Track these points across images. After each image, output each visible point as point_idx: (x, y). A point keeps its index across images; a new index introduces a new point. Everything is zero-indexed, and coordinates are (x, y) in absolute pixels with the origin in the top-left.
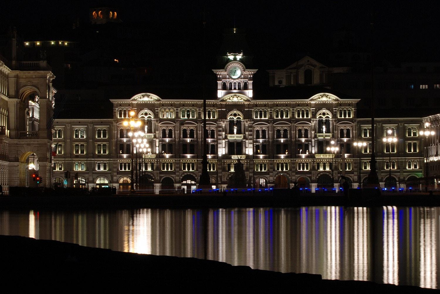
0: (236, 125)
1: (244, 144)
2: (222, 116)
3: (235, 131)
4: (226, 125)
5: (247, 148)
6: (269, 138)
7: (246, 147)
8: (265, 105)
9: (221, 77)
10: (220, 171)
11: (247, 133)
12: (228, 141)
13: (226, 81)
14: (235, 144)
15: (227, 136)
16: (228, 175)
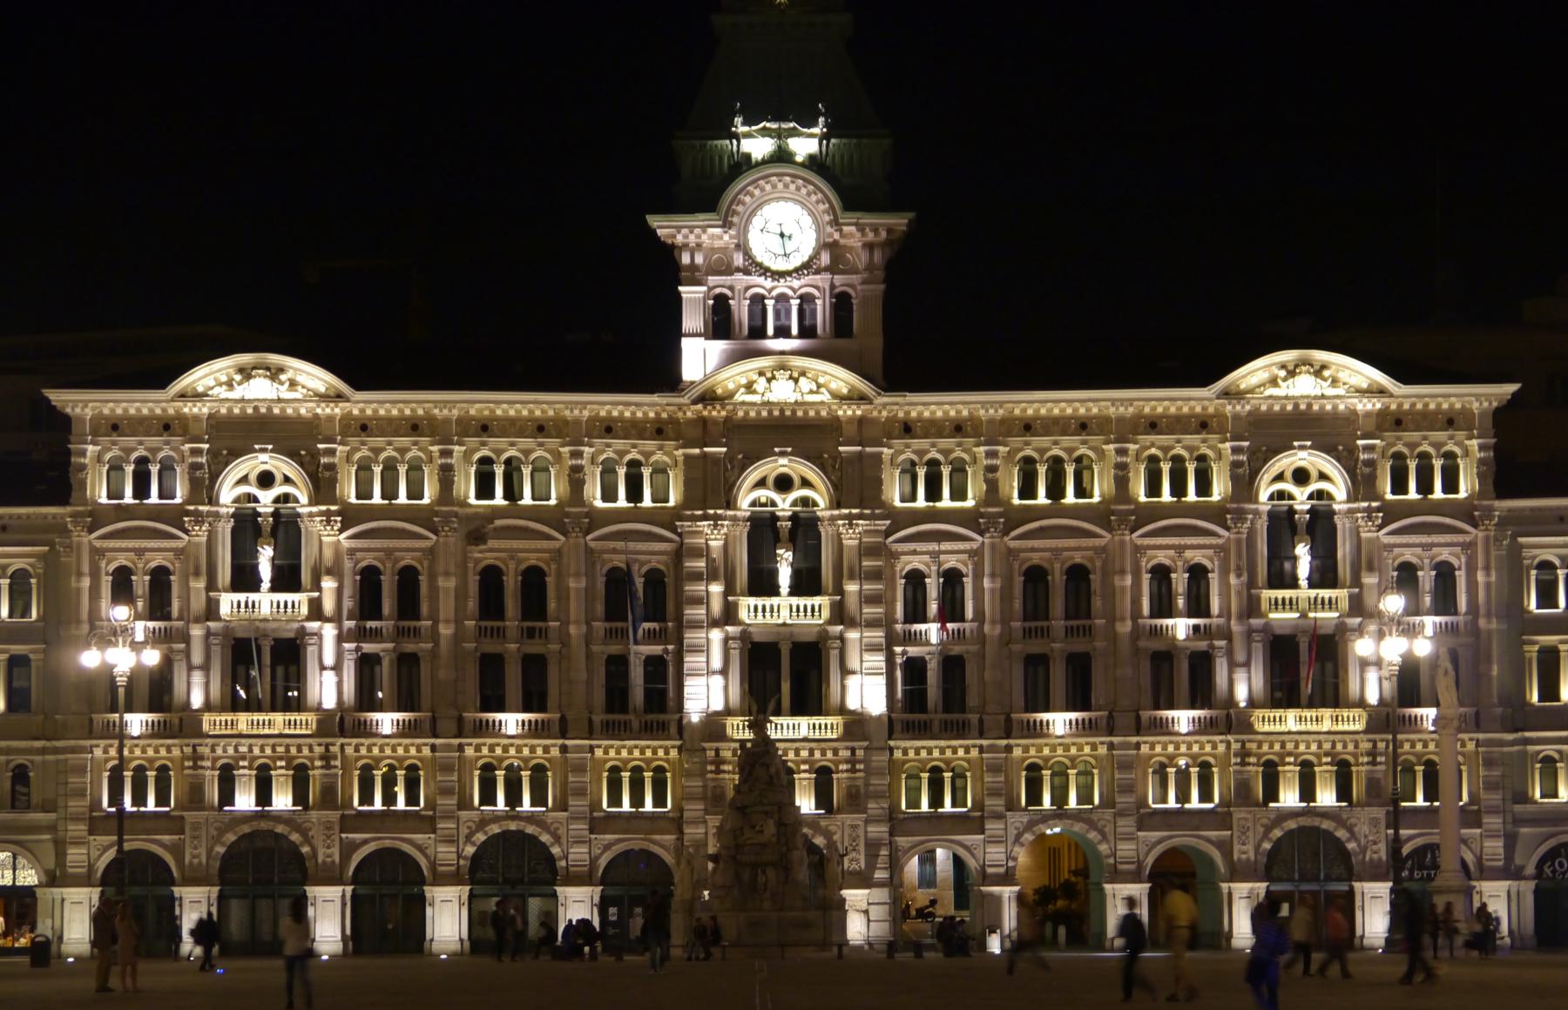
0: (793, 540)
1: (834, 654)
2: (711, 489)
4: (730, 540)
5: (854, 673)
6: (979, 616)
7: (846, 672)
9: (699, 259)
11: (851, 588)
13: (731, 288)
15: (736, 605)
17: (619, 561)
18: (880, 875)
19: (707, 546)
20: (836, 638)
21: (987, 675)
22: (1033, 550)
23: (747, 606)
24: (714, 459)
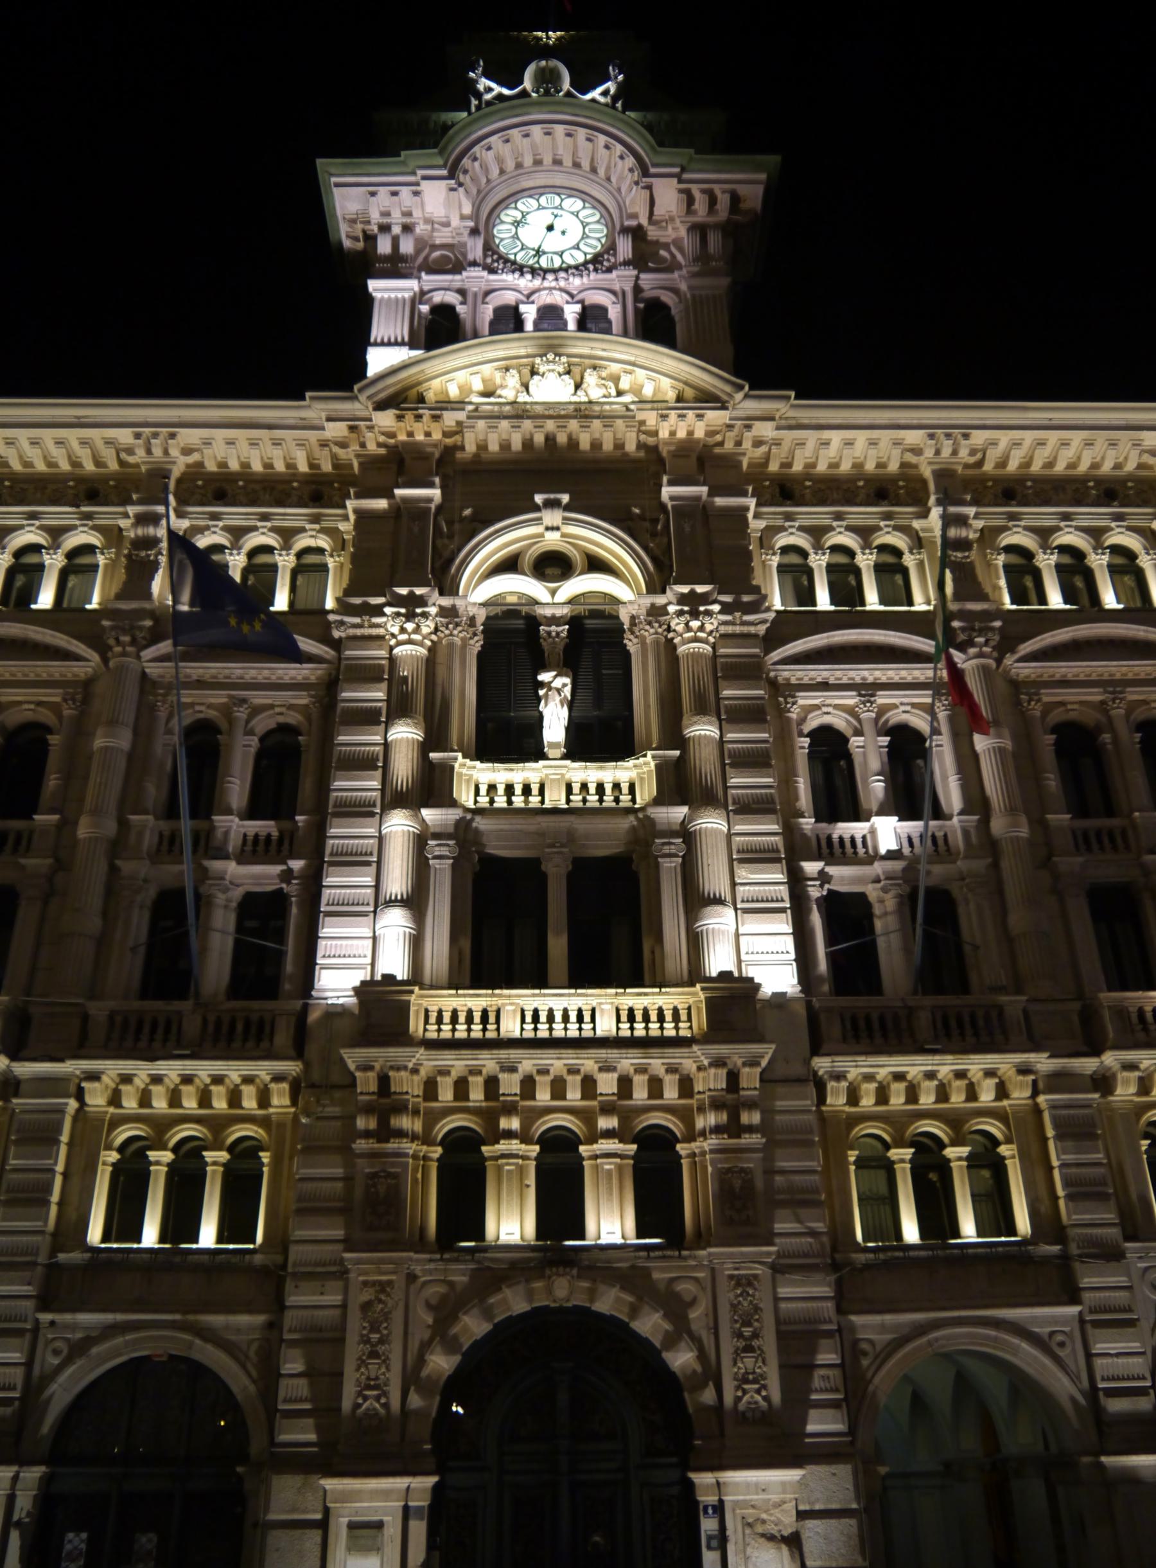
0: (569, 663)
1: (670, 866)
2: (409, 555)
3: (555, 722)
4: (441, 658)
5: (719, 901)
6: (976, 801)
7: (697, 900)
8: (887, 490)
9: (407, 247)
10: (319, 1237)
11: (702, 730)
12: (463, 833)
13: (462, 292)
14: (556, 871)
15: (447, 770)
16: (446, 1312)
17: (206, 704)
18: (822, 1424)
19: (392, 659)
20: (673, 834)
21: (1018, 920)
22: (1064, 683)
23: (477, 779)
24: (415, 511)
